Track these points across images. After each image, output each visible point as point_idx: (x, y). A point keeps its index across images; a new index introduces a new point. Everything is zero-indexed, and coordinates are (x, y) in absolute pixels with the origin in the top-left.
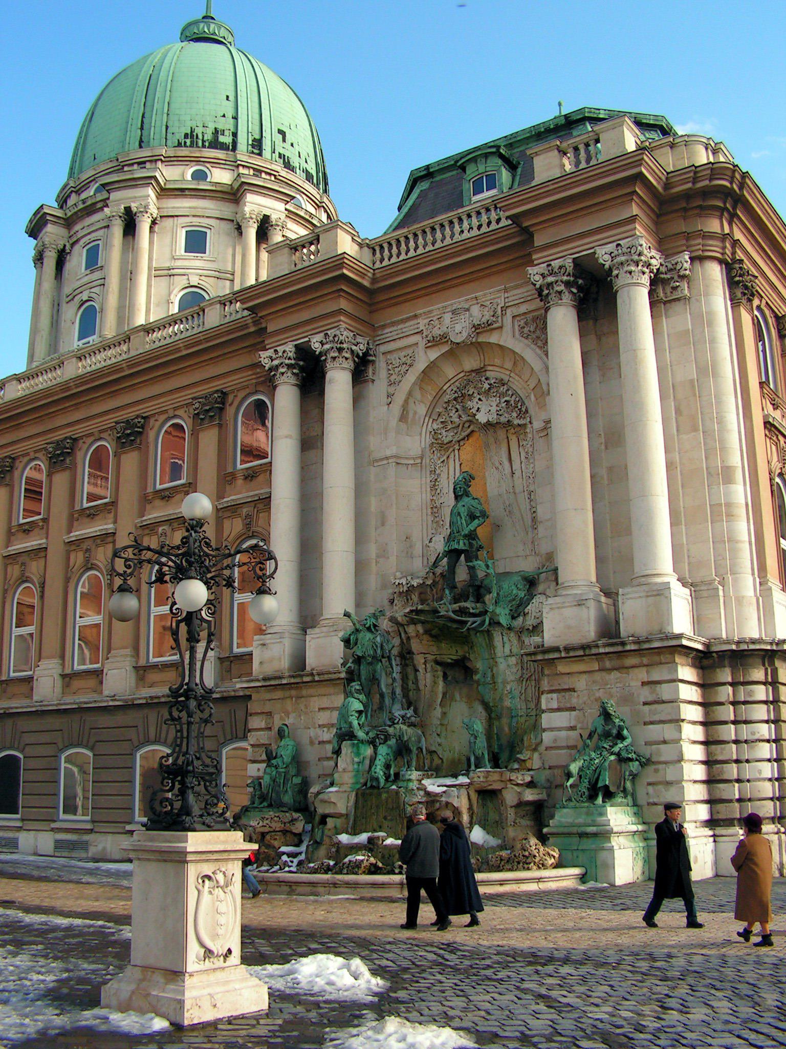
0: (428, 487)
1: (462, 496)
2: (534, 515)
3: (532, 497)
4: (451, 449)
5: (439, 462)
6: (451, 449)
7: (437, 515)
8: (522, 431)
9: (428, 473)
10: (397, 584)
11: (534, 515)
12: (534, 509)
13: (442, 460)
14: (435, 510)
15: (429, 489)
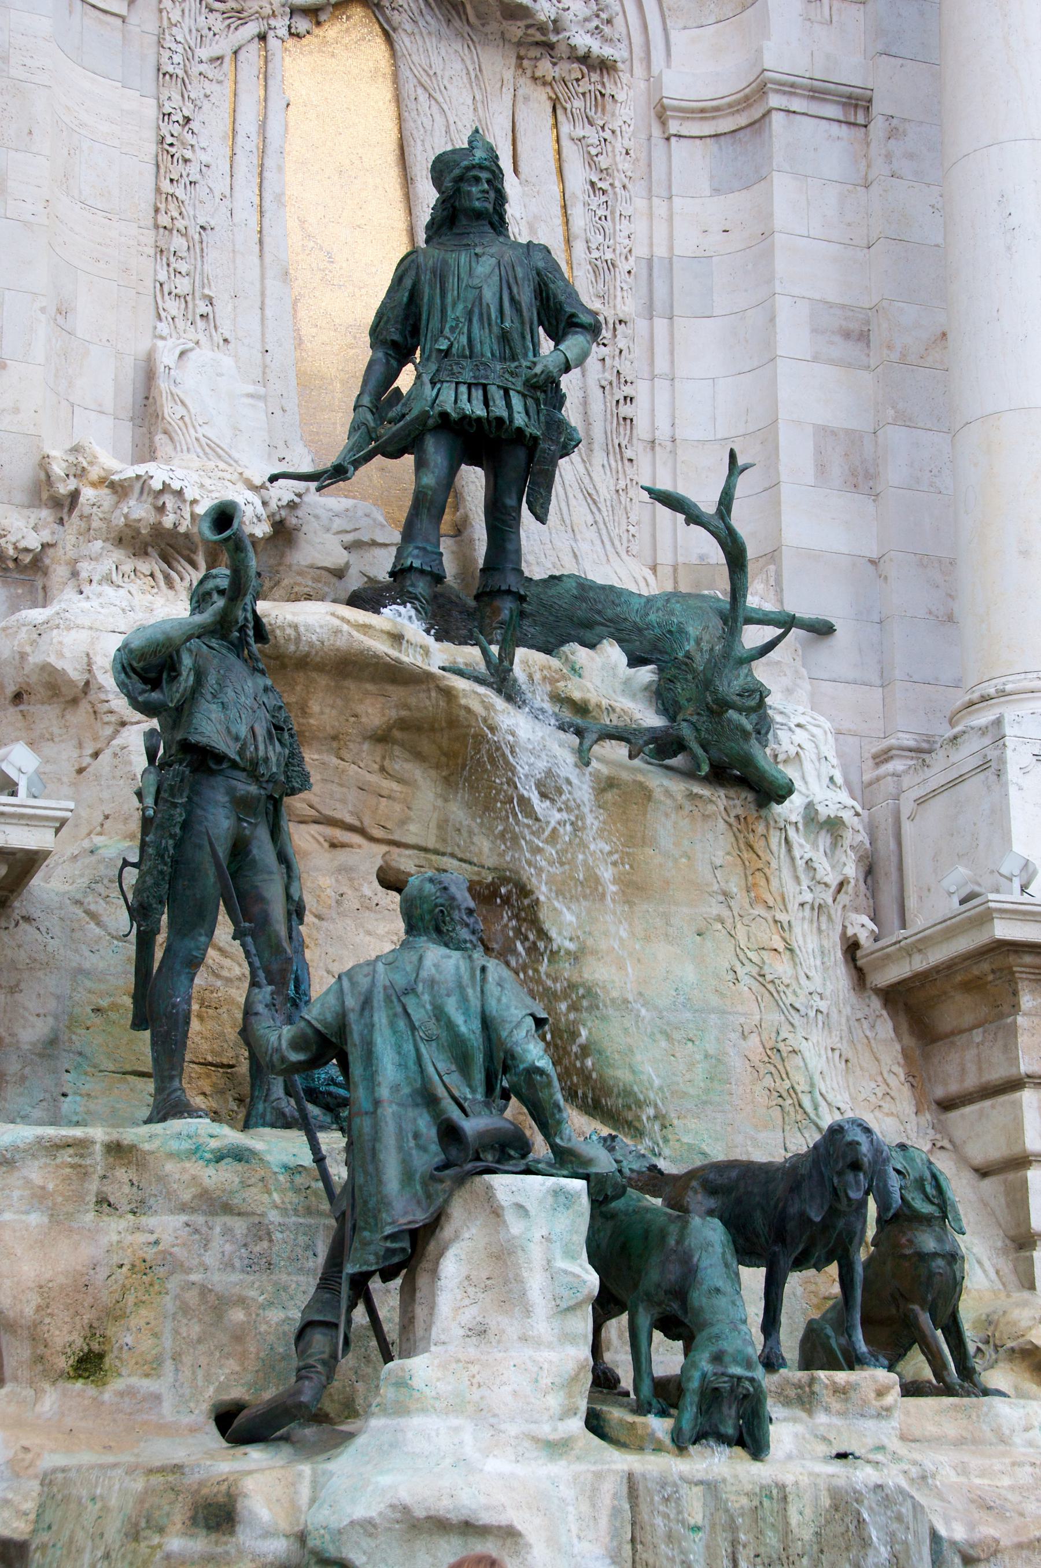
0: (151, 136)
1: (478, 215)
2: (625, 410)
3: (622, 343)
4: (252, 28)
5: (204, 53)
6: (252, 28)
7: (183, 267)
8: (584, 86)
9: (151, 73)
10: (156, 485)
11: (625, 410)
12: (628, 390)
13: (215, 50)
14: (178, 243)
15: (151, 148)
